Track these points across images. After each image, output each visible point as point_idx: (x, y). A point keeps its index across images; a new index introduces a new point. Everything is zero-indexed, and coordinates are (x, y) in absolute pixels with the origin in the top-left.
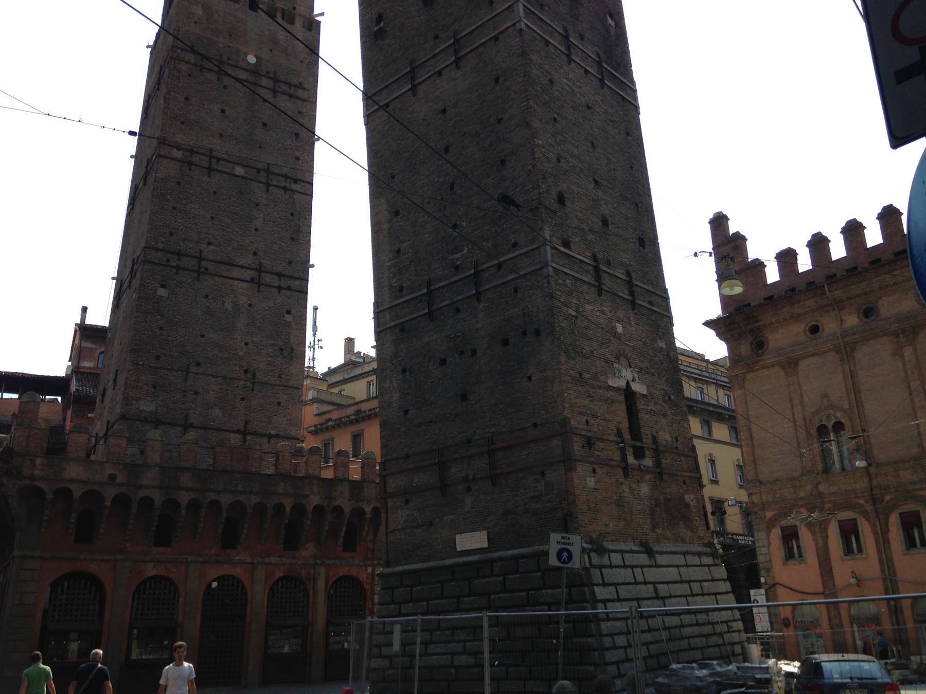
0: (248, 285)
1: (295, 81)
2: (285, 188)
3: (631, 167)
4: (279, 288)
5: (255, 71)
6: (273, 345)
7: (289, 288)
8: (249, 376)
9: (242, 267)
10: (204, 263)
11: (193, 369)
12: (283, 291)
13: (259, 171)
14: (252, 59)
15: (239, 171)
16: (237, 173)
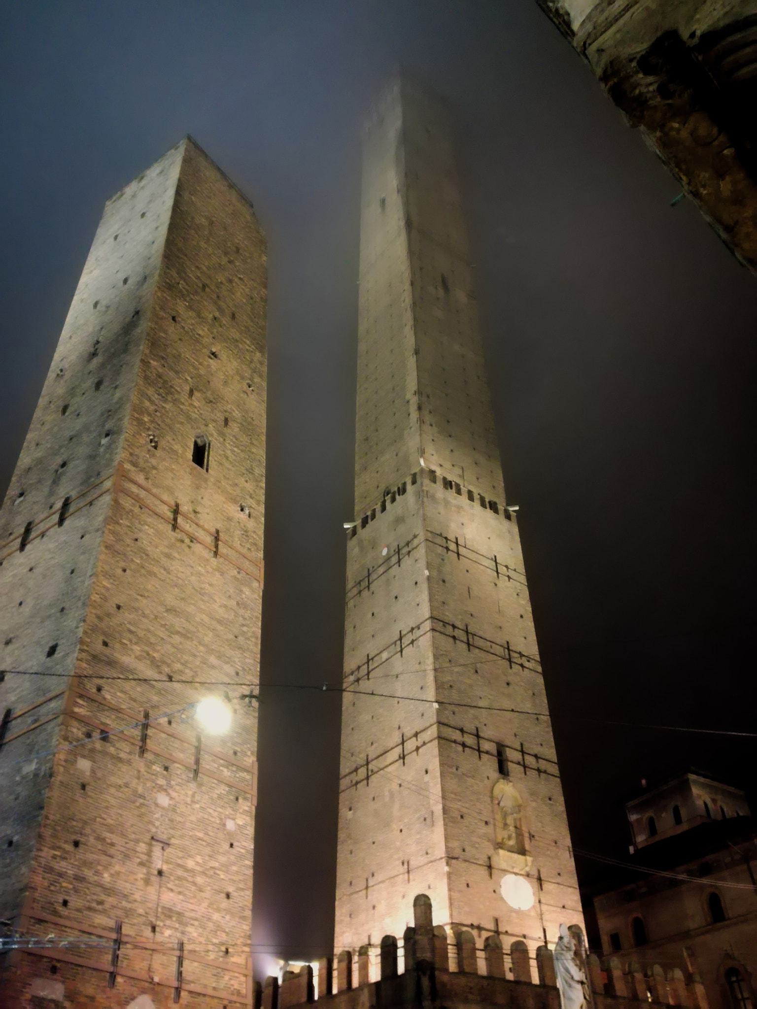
0: (397, 764)
1: (411, 537)
2: (412, 642)
3: (72, 572)
4: (418, 749)
5: (388, 558)
6: (419, 818)
7: (424, 744)
8: (406, 866)
9: (392, 748)
10: (370, 767)
11: (370, 884)
12: (420, 750)
13: (395, 643)
14: (385, 552)
15: (385, 655)
16: (383, 660)
